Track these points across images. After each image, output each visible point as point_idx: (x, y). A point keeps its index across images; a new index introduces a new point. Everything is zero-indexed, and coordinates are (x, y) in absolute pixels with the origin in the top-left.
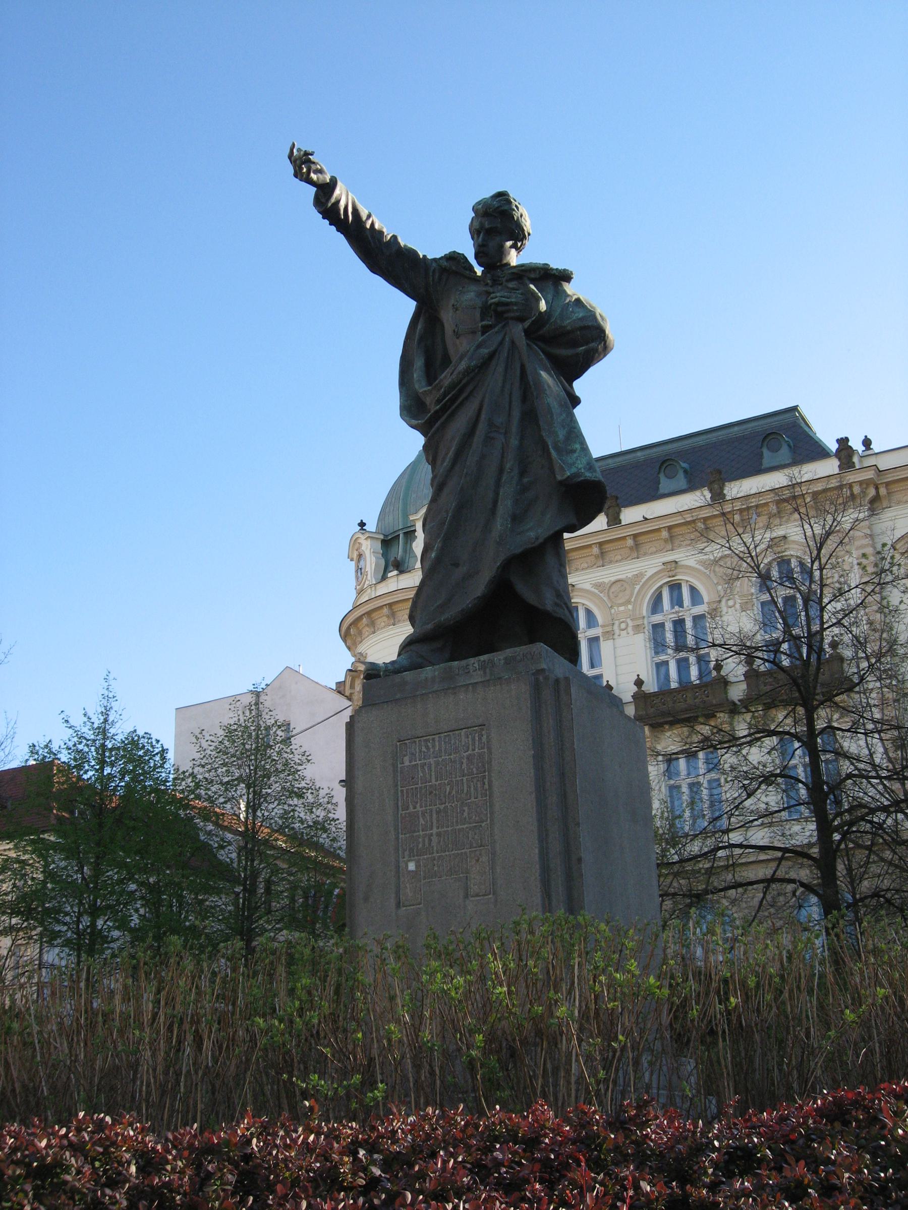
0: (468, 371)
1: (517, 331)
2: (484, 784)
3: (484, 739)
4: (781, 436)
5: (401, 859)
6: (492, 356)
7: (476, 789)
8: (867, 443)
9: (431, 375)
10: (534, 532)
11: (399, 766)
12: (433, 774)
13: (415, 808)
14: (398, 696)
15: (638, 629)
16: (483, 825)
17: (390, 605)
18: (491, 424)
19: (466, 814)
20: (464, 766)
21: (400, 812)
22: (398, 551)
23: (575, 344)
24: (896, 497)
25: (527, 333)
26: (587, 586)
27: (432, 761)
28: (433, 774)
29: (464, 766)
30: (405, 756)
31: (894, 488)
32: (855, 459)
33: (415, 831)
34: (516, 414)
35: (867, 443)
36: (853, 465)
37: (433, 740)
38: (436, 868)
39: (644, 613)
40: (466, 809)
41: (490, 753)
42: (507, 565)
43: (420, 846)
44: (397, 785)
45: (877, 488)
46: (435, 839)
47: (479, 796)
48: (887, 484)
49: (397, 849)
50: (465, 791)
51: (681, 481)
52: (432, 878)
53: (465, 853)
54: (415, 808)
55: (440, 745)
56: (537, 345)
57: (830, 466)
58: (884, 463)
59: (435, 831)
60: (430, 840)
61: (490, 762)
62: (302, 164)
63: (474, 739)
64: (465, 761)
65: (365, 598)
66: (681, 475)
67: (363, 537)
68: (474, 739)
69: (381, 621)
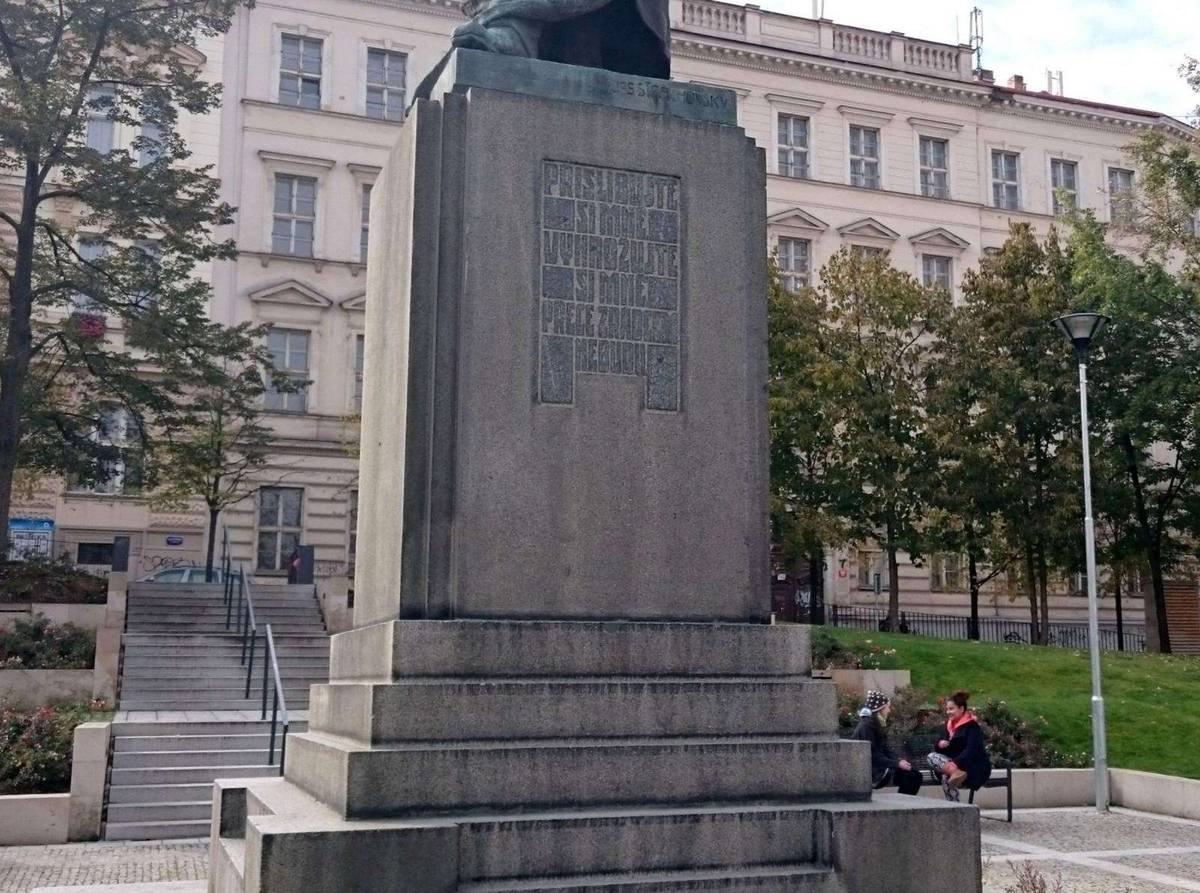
2: (674, 257)
3: (677, 196)
5: (541, 334)
7: (661, 261)
11: (543, 195)
12: (597, 222)
13: (566, 263)
14: (520, 89)
16: (670, 313)
19: (645, 293)
20: (646, 225)
21: (543, 263)
27: (597, 203)
28: (597, 222)
29: (646, 225)
30: (554, 183)
33: (565, 297)
37: (600, 174)
38: (596, 358)
40: (646, 285)
41: (685, 220)
43: (573, 321)
44: (538, 223)
46: (596, 317)
47: (666, 272)
49: (535, 316)
50: (646, 261)
52: (590, 369)
53: (643, 346)
54: (566, 263)
55: (609, 183)
59: (597, 303)
60: (589, 316)
61: (685, 231)
63: (660, 192)
64: (646, 219)
68: (660, 192)
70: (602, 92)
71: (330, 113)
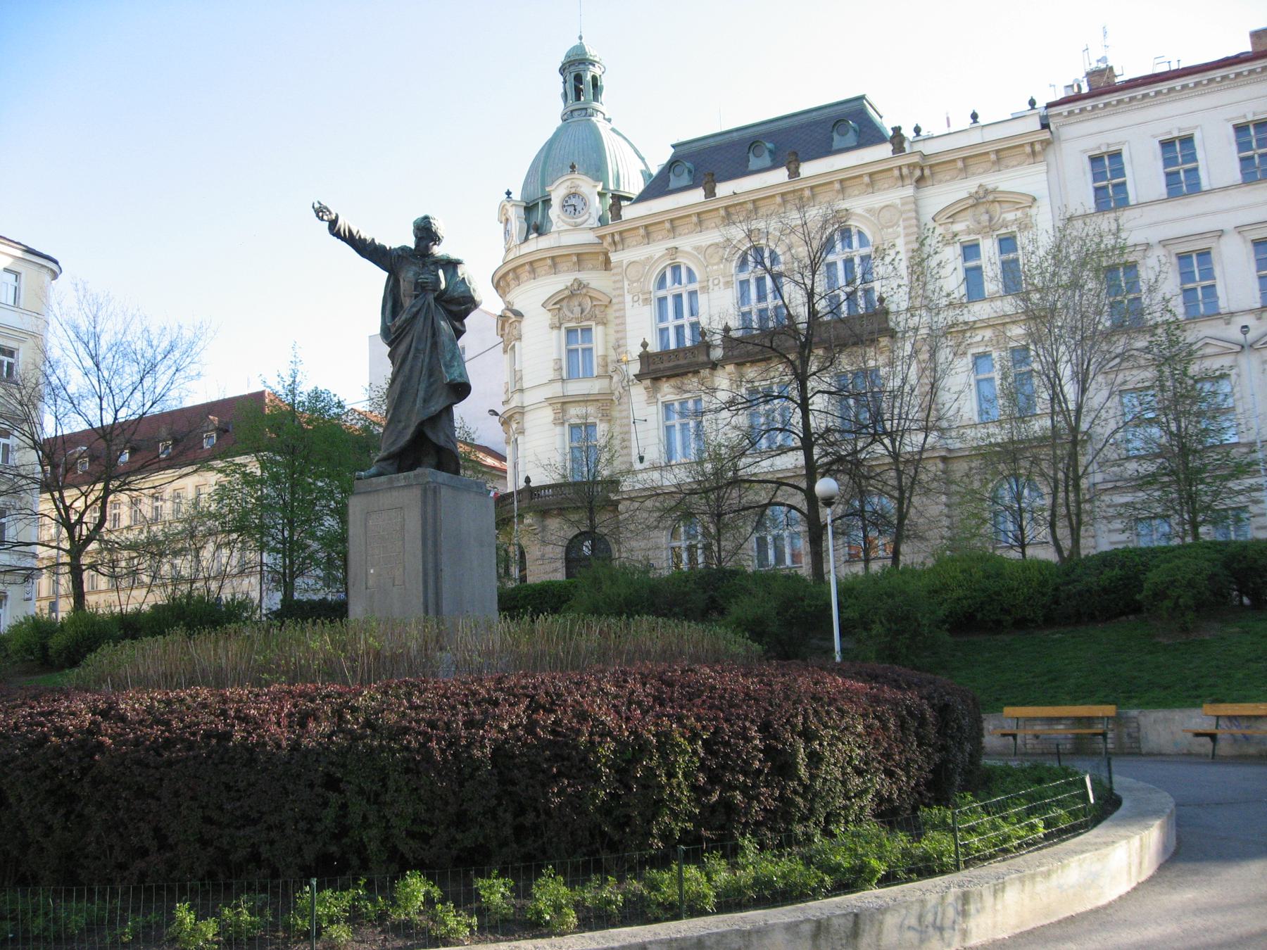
0: (405, 321)
1: (431, 298)
4: (846, 124)
6: (418, 312)
8: (917, 130)
9: (394, 314)
10: (435, 408)
15: (728, 284)
17: (531, 263)
18: (417, 349)
22: (538, 216)
23: (461, 304)
24: (939, 176)
25: (436, 299)
26: (688, 249)
31: (937, 169)
32: (906, 145)
34: (429, 344)
35: (917, 130)
36: (902, 150)
39: (733, 271)
42: (422, 424)
45: (922, 170)
48: (931, 166)
51: (766, 160)
56: (443, 307)
57: (885, 150)
58: (928, 148)
62: (320, 211)
65: (511, 256)
66: (766, 153)
67: (508, 206)
69: (524, 275)
70: (391, 481)
71: (1138, 205)
